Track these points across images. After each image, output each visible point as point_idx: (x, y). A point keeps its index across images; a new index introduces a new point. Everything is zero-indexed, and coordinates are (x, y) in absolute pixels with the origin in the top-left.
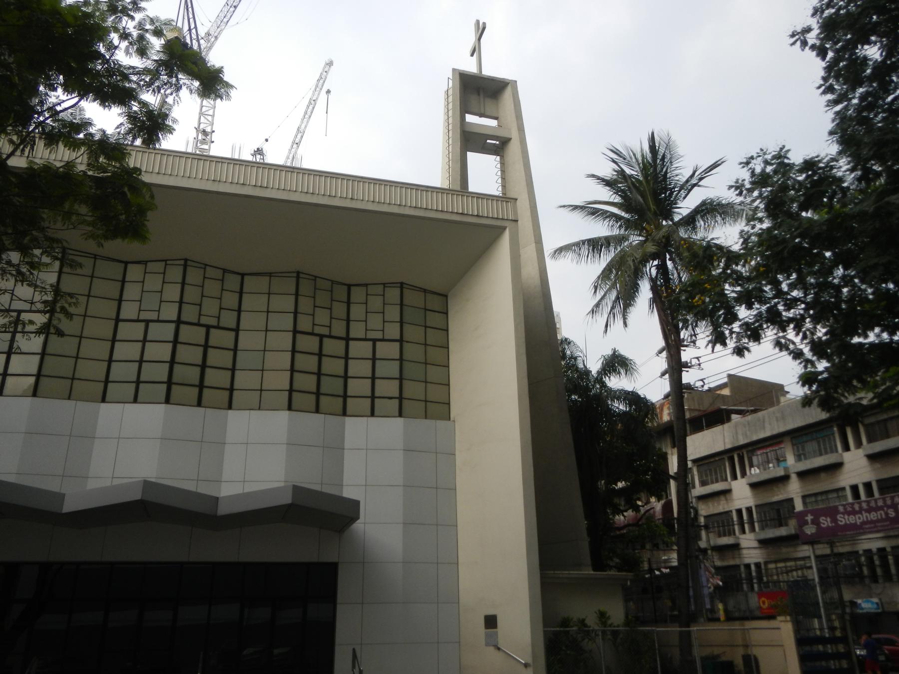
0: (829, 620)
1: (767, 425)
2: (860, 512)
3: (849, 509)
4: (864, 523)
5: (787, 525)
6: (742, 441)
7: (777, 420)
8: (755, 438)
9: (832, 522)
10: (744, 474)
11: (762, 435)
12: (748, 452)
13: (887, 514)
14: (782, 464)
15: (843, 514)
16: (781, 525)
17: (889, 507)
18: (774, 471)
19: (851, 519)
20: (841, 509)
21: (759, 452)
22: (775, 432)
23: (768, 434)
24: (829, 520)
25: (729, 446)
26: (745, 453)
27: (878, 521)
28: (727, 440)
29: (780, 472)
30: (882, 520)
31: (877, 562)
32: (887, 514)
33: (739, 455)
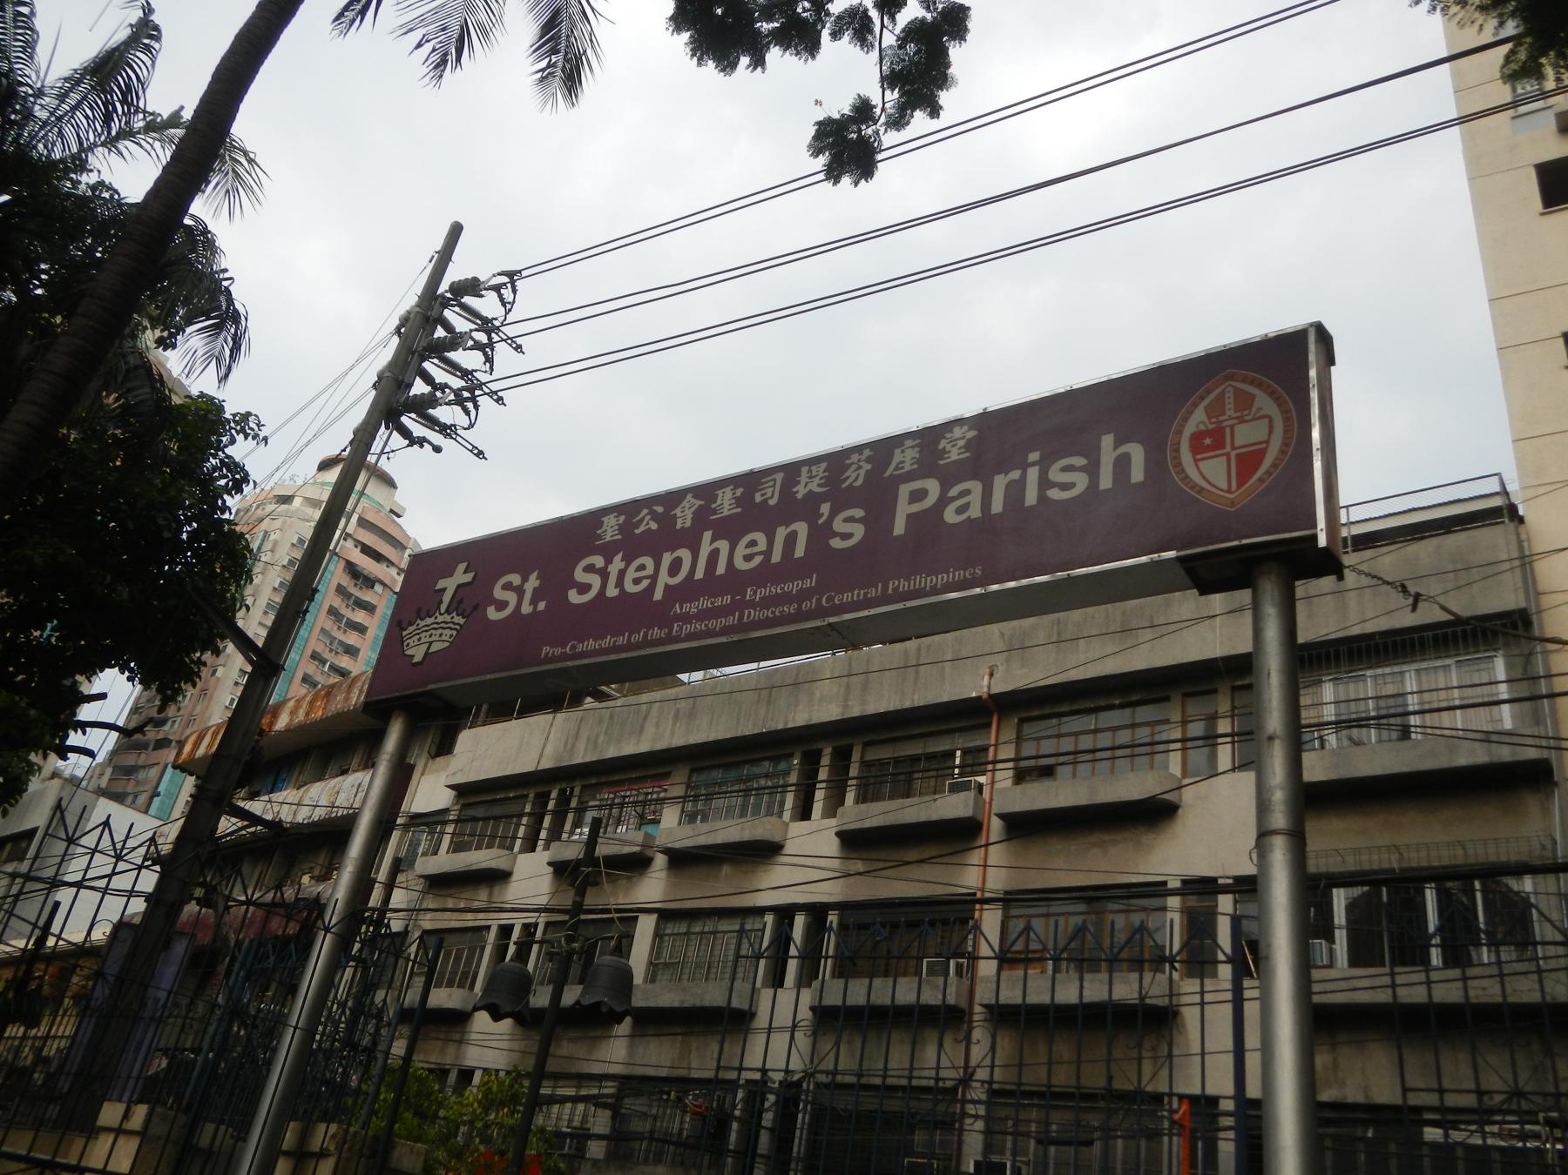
1: (650, 729)
4: (689, 590)
6: (581, 756)
8: (612, 752)
10: (555, 835)
11: (629, 748)
12: (584, 787)
13: (821, 534)
14: (650, 829)
20: (610, 530)
22: (661, 745)
23: (644, 747)
24: (533, 582)
25: (546, 764)
26: (577, 791)
28: (549, 750)
31: (768, 1118)
33: (562, 791)
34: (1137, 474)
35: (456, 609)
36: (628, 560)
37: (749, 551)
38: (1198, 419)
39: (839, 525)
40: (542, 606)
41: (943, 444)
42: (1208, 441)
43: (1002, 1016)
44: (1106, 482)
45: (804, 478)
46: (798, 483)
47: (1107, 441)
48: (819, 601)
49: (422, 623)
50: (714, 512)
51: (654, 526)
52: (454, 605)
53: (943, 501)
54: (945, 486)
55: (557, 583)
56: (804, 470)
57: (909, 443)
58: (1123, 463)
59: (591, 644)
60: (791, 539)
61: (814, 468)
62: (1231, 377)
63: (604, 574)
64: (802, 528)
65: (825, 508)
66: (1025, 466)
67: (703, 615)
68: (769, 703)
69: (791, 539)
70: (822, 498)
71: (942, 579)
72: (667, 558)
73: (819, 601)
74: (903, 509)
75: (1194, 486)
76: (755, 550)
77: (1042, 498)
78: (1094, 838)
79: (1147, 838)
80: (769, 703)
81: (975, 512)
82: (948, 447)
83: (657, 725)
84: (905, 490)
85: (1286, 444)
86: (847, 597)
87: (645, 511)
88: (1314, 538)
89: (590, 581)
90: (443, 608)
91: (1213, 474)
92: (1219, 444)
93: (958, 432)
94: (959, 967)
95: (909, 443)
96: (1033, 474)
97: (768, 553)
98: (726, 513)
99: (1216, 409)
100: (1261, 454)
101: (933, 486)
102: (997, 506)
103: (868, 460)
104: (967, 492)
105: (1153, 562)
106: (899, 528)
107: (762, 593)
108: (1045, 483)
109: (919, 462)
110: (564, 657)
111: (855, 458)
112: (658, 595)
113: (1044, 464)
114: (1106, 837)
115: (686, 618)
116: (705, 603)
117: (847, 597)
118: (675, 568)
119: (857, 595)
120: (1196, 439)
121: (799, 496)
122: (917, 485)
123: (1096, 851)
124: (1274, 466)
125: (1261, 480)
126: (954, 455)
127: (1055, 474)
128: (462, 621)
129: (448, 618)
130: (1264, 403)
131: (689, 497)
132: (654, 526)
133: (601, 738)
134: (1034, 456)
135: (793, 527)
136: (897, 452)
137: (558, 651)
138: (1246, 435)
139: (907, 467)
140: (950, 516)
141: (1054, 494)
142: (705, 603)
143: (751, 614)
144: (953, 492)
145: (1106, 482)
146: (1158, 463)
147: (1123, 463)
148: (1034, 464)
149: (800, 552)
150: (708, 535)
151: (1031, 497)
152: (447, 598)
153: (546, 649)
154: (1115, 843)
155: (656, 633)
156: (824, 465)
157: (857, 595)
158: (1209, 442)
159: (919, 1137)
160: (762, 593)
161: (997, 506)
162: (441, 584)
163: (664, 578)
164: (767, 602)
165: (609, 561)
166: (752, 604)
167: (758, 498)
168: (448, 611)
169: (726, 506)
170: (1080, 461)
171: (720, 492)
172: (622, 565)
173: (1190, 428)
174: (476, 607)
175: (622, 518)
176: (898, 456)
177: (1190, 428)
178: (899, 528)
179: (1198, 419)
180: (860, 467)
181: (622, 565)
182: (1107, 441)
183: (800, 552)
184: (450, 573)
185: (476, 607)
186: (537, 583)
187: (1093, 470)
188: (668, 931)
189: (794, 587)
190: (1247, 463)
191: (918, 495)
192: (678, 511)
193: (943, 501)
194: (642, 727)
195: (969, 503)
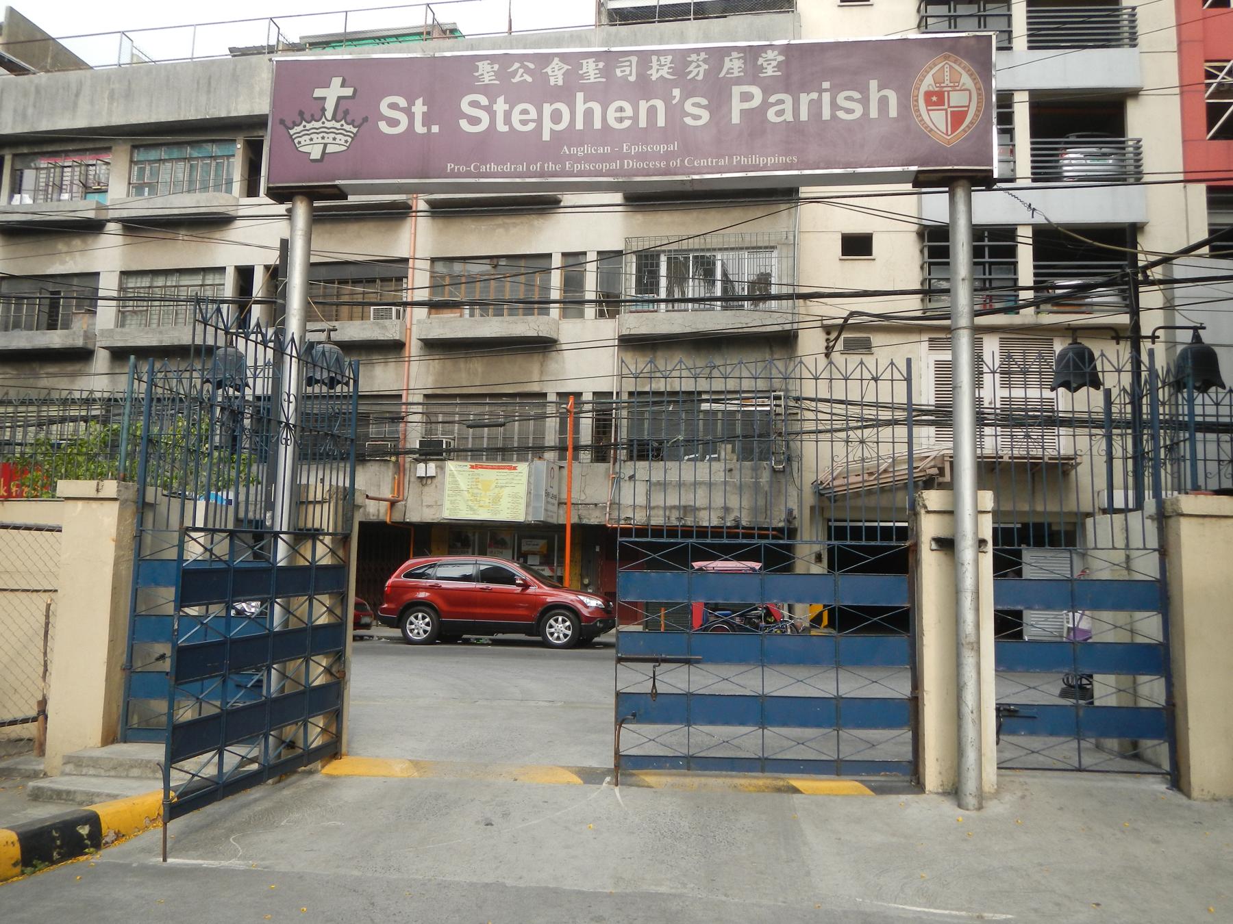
0: (300, 501)
1: (83, 104)
2: (565, 93)
3: (521, 77)
5: (66, 326)
7: (112, 97)
9: (427, 122)
12: (15, 156)
13: (675, 113)
14: (93, 199)
16: (52, 326)
18: (71, 205)
19: (521, 118)
20: (486, 73)
21: (43, 163)
23: (81, 122)
24: (419, 108)
29: (85, 209)
32: (675, 113)
34: (893, 113)
35: (344, 118)
37: (619, 115)
39: (688, 107)
40: (435, 129)
41: (761, 61)
42: (934, 99)
43: (433, 346)
44: (874, 113)
45: (655, 64)
46: (651, 68)
47: (874, 84)
48: (682, 161)
49: (309, 126)
50: (582, 77)
51: (529, 79)
52: (340, 115)
53: (765, 105)
54: (767, 92)
55: (443, 108)
56: (654, 58)
57: (735, 54)
58: (883, 102)
59: (493, 167)
60: (652, 111)
61: (662, 58)
62: (946, 58)
63: (489, 109)
64: (660, 104)
65: (676, 92)
66: (821, 91)
67: (588, 158)
68: (209, 92)
69: (652, 111)
70: (674, 84)
71: (771, 161)
72: (547, 109)
73: (682, 161)
75: (927, 127)
76: (624, 114)
77: (834, 116)
78: (500, 220)
79: (538, 221)
80: (209, 92)
81: (789, 116)
82: (765, 65)
83: (92, 103)
84: (736, 91)
85: (978, 110)
86: (703, 162)
87: (517, 65)
88: (991, 171)
89: (476, 115)
90: (329, 114)
91: (937, 120)
93: (770, 54)
94: (398, 312)
96: (826, 97)
97: (635, 118)
98: (592, 80)
101: (756, 91)
102: (804, 116)
103: (705, 61)
104: (781, 102)
105: (903, 172)
106: (736, 119)
108: (834, 106)
109: (744, 71)
110: (468, 174)
112: (546, 137)
113: (834, 91)
114: (508, 220)
115: (578, 160)
116: (588, 149)
117: (703, 162)
118: (556, 117)
119: (710, 162)
120: (928, 95)
121: (654, 78)
122: (746, 88)
123: (501, 230)
124: (971, 123)
125: (964, 130)
126: (770, 71)
127: (840, 100)
128: (355, 130)
129: (338, 125)
130: (966, 80)
131: (556, 60)
132: (529, 79)
133: (30, 111)
134: (826, 85)
135: (652, 102)
136: (727, 59)
137: (463, 169)
138: (957, 99)
139: (736, 74)
140: (771, 115)
142: (588, 149)
143: (629, 164)
144: (772, 99)
145: (874, 113)
146: (904, 106)
147: (883, 102)
148: (826, 90)
149: (661, 122)
150: (580, 96)
151: (826, 115)
152: (330, 106)
153: (450, 166)
154: (515, 225)
155: (551, 166)
156: (670, 58)
157: (710, 162)
158: (936, 98)
159: (372, 430)
161: (804, 116)
162: (318, 93)
163: (547, 125)
164: (642, 157)
165: (493, 101)
166: (628, 156)
167: (618, 73)
168: (334, 118)
169: (592, 77)
170: (857, 95)
171: (584, 62)
172: (507, 107)
173: (924, 88)
174: (365, 120)
175: (496, 67)
176: (727, 64)
178: (736, 119)
179: (928, 83)
180: (699, 66)
181: (507, 107)
182: (874, 84)
183: (661, 122)
185: (365, 120)
186: (425, 109)
187: (865, 102)
188: (130, 285)
189: (662, 148)
190: (957, 118)
191: (746, 97)
192: (549, 70)
193: (765, 105)
194: (75, 105)
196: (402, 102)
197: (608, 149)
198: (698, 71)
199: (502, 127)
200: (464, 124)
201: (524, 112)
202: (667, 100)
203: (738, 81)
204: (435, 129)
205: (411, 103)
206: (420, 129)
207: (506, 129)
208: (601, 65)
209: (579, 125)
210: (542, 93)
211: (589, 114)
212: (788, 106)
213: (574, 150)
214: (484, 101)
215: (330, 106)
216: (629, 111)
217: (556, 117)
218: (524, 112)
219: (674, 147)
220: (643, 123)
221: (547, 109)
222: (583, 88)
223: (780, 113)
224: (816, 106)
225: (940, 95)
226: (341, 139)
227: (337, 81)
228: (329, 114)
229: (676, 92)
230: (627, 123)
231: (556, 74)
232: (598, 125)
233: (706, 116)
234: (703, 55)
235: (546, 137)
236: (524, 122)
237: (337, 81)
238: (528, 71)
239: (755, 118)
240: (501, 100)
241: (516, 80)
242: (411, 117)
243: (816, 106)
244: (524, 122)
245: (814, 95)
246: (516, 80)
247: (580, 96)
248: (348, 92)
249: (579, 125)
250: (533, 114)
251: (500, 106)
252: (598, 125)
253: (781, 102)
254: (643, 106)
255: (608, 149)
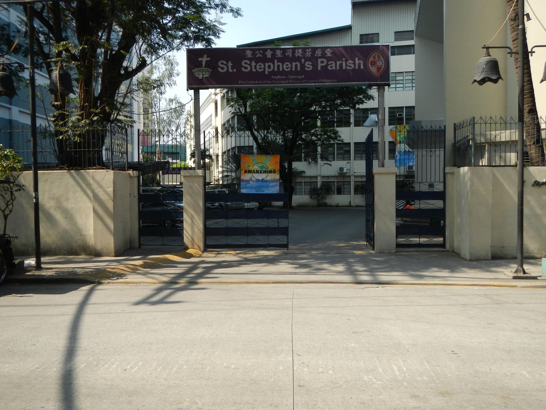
2: (272, 60)
9: (232, 68)
13: (303, 66)
15: (251, 60)
17: (307, 59)
19: (260, 67)
20: (249, 53)
24: (230, 64)
27: (291, 72)
30: (296, 73)
36: (257, 63)
38: (371, 59)
41: (326, 52)
47: (357, 59)
50: (276, 55)
53: (327, 65)
55: (237, 65)
60: (296, 66)
63: (250, 65)
65: (303, 60)
69: (296, 66)
72: (267, 65)
74: (320, 65)
81: (334, 68)
84: (319, 60)
90: (204, 65)
92: (375, 64)
93: (329, 50)
95: (319, 50)
97: (292, 68)
99: (374, 58)
100: (381, 68)
101: (324, 60)
102: (338, 68)
104: (332, 64)
106: (319, 68)
107: (292, 77)
108: (346, 65)
111: (307, 50)
112: (267, 73)
116: (279, 77)
118: (269, 67)
120: (371, 62)
138: (379, 63)
140: (329, 68)
141: (348, 68)
142: (279, 77)
144: (329, 63)
146: (365, 65)
149: (299, 69)
150: (276, 61)
152: (204, 63)
158: (373, 63)
160: (292, 77)
162: (200, 59)
163: (267, 70)
165: (251, 62)
166: (290, 79)
176: (317, 52)
177: (370, 60)
178: (319, 68)
182: (357, 59)
183: (299, 69)
184: (202, 57)
187: (354, 64)
190: (379, 69)
191: (322, 62)
192: (266, 53)
193: (327, 65)
195: (333, 66)
196: (225, 63)
197: (284, 77)
198: (308, 54)
199: (254, 70)
200: (243, 69)
201: (260, 65)
202: (300, 62)
203: (320, 57)
204: (235, 70)
205: (227, 63)
206: (230, 70)
207: (255, 70)
208: (282, 52)
209: (276, 70)
210: (264, 60)
211: (278, 66)
212: (334, 65)
213: (275, 77)
214: (248, 62)
215: (204, 63)
216: (290, 66)
217: (269, 67)
218: (260, 65)
219: (303, 77)
220: (294, 69)
221: (267, 65)
222: (276, 58)
223: (331, 67)
224: (341, 65)
225: (375, 62)
226: (207, 73)
227: (205, 56)
228: (204, 65)
229: (303, 60)
230: (289, 69)
231: (269, 54)
232: (281, 69)
233: (311, 67)
234: (310, 50)
235: (267, 73)
236: (260, 69)
237: (205, 56)
238: (261, 53)
239: (325, 68)
240: (253, 62)
241: (257, 56)
242: (228, 67)
243: (341, 65)
244: (260, 69)
245: (341, 62)
246: (257, 56)
247: (276, 61)
248: (209, 59)
249: (276, 70)
250: (263, 66)
251: (253, 64)
252: (281, 69)
253: (332, 64)
254: (294, 64)
255: (284, 77)
